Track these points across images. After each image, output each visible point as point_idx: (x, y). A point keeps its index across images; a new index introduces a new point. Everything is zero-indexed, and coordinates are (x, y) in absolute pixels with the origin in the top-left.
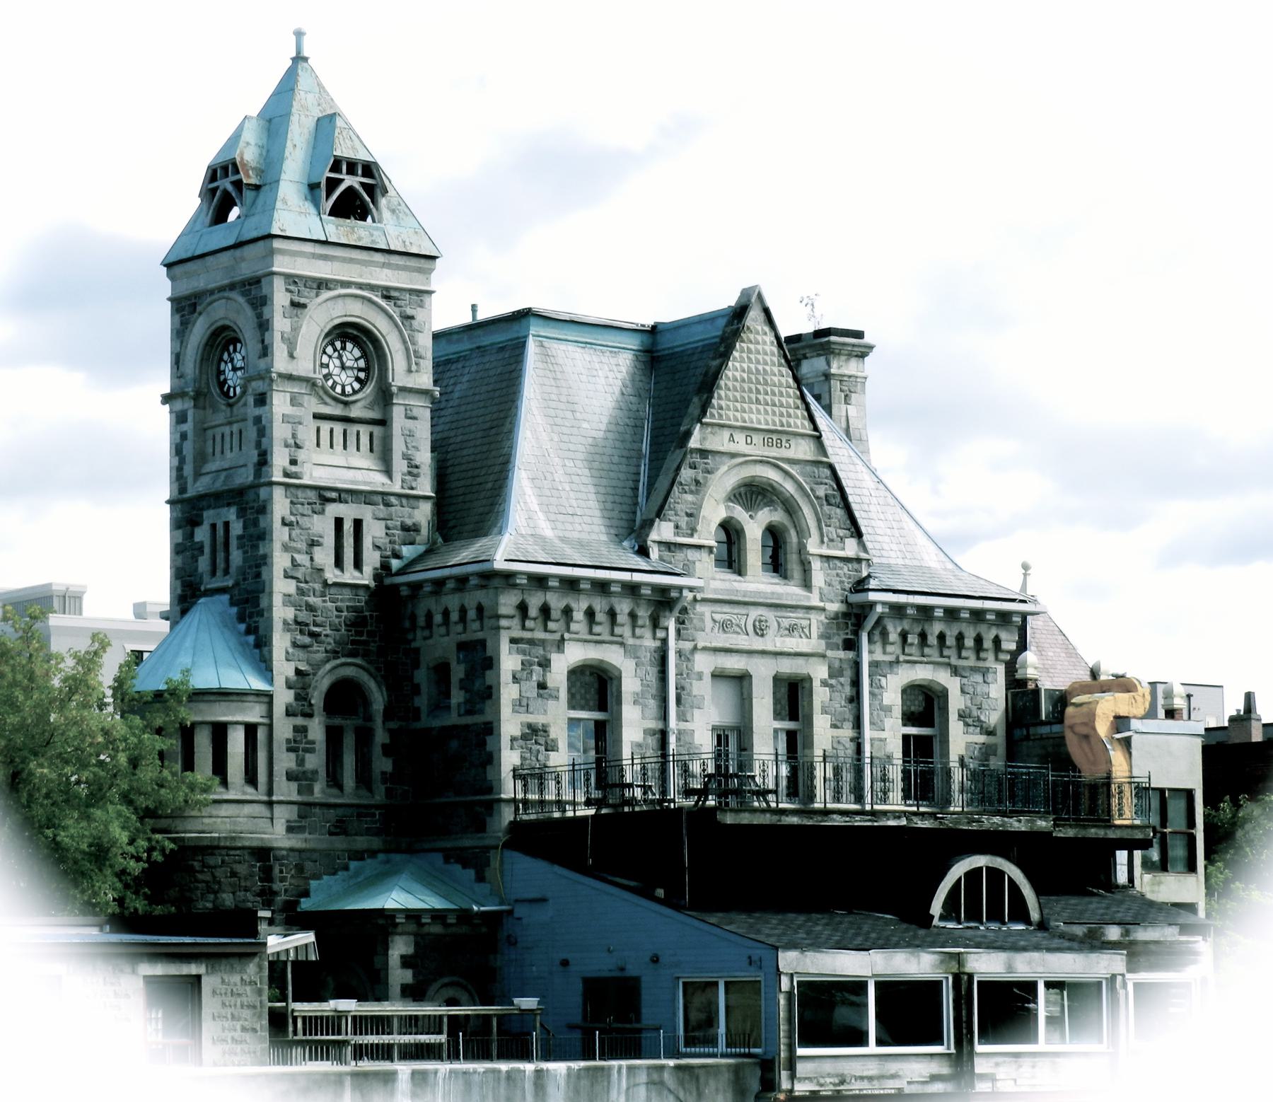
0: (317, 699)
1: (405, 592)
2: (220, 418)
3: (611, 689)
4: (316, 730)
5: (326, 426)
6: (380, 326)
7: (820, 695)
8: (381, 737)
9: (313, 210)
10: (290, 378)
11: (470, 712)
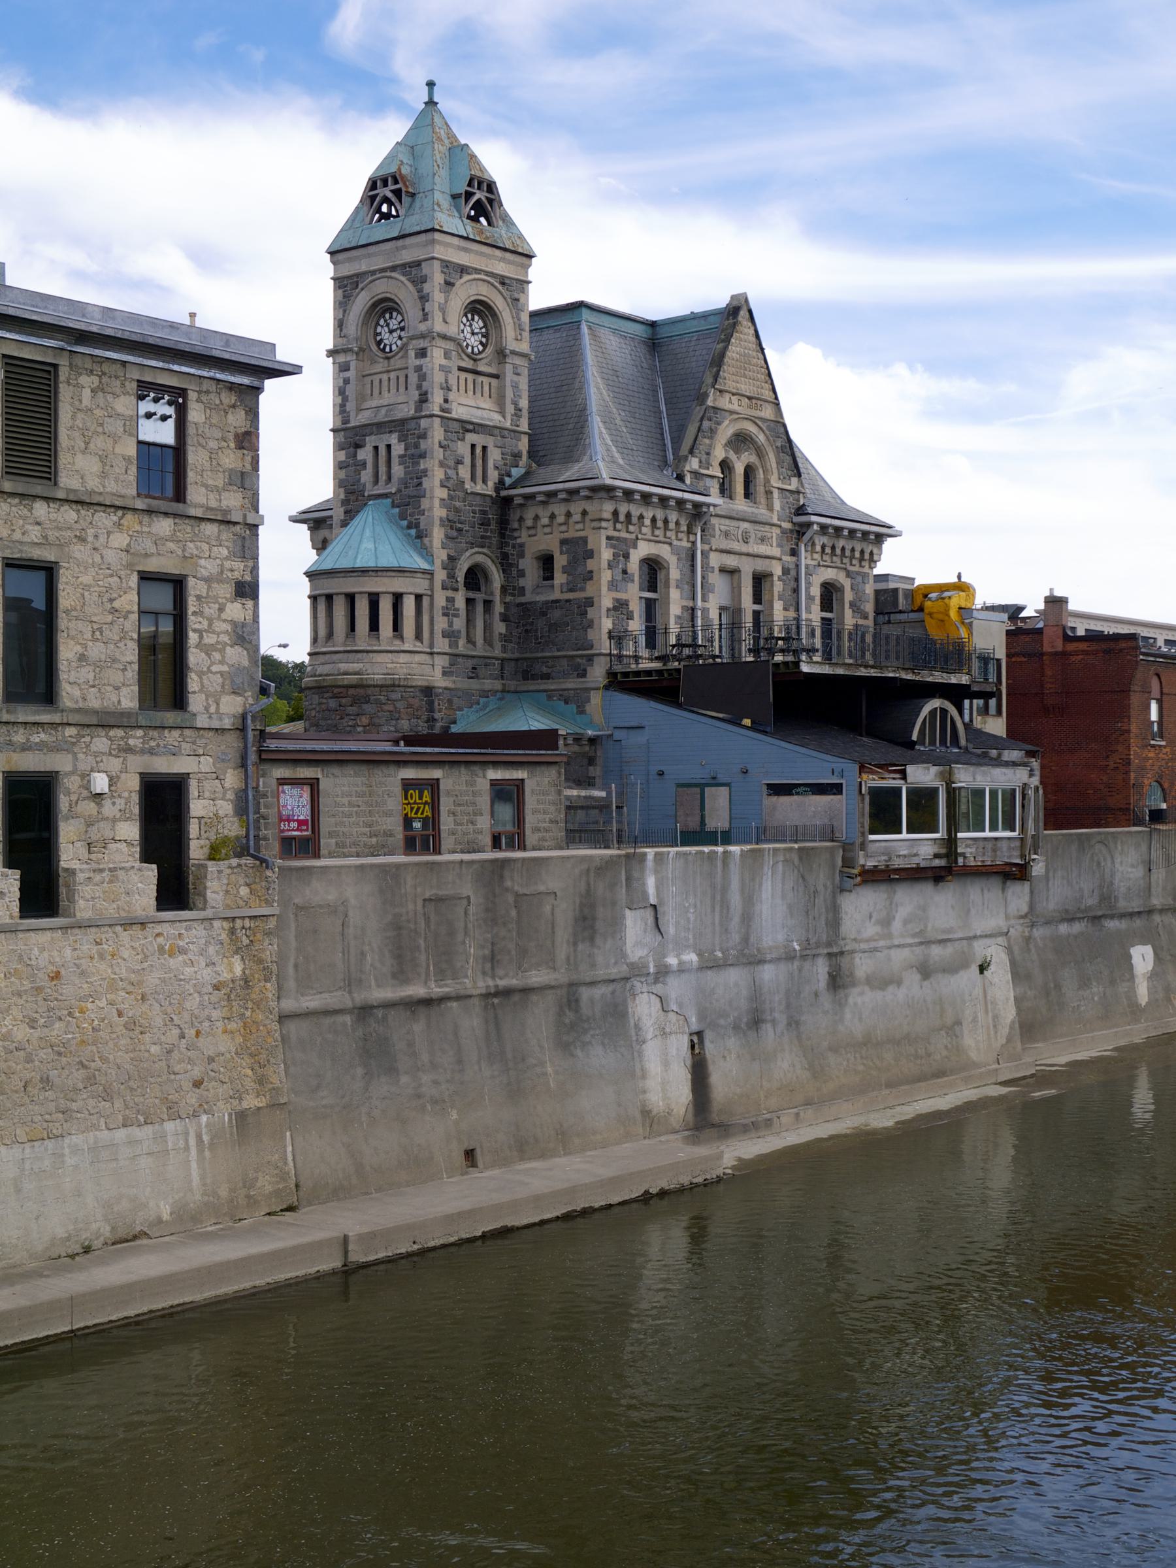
0: (461, 576)
1: (518, 501)
2: (379, 368)
3: (661, 576)
4: (460, 603)
5: (463, 375)
6: (499, 303)
7: (778, 586)
8: (498, 608)
9: (457, 214)
10: (444, 337)
11: (571, 590)
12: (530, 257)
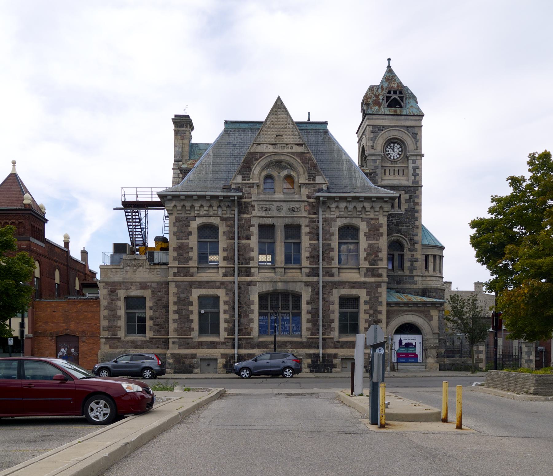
12: (423, 116)
